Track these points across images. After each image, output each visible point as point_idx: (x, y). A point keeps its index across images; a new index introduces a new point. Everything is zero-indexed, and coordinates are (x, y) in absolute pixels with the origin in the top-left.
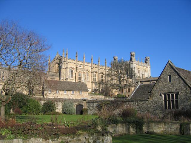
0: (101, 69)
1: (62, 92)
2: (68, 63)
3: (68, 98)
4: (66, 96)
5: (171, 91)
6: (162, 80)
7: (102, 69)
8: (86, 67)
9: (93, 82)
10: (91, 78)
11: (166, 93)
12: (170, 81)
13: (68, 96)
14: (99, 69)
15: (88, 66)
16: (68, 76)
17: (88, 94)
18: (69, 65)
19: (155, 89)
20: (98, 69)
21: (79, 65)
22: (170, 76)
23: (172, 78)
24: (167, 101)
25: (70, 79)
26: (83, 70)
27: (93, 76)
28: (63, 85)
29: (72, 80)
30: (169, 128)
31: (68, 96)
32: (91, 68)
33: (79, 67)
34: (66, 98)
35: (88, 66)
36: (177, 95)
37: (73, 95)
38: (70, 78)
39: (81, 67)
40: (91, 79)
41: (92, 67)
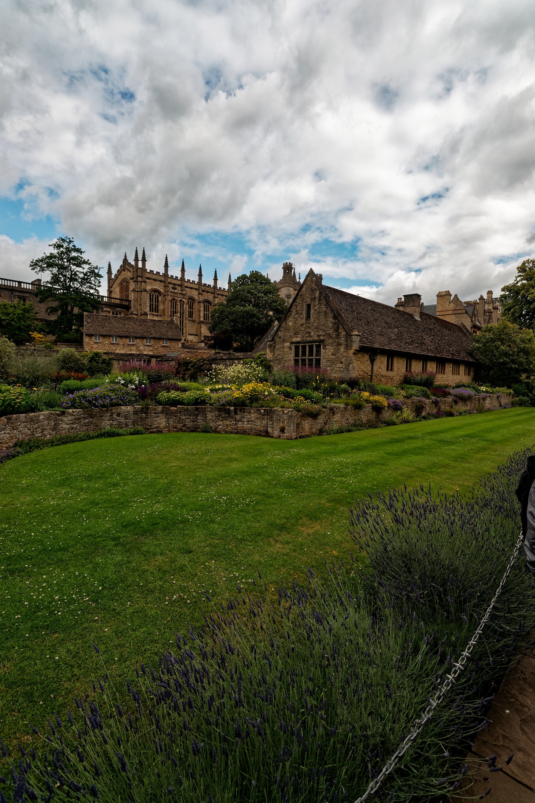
0: (220, 296)
1: (121, 341)
2: (147, 280)
3: (138, 353)
4: (133, 348)
5: (308, 339)
6: (293, 314)
7: (222, 295)
8: (187, 289)
9: (202, 322)
10: (197, 314)
11: (299, 342)
12: (308, 317)
13: (138, 348)
14: (216, 295)
15: (191, 288)
16: (148, 308)
17: (180, 345)
18: (150, 284)
19: (280, 333)
20: (213, 295)
21: (172, 286)
22: (309, 306)
23: (312, 311)
24: (300, 360)
25: (153, 315)
26: (181, 296)
27: (202, 309)
28: (127, 326)
29: (157, 315)
30: (245, 420)
31: (138, 348)
32: (199, 294)
33: (173, 291)
34: (135, 353)
35: (191, 288)
36: (318, 347)
37: (149, 346)
38: (154, 313)
39: (176, 291)
40: (197, 317)
41: (201, 291)
